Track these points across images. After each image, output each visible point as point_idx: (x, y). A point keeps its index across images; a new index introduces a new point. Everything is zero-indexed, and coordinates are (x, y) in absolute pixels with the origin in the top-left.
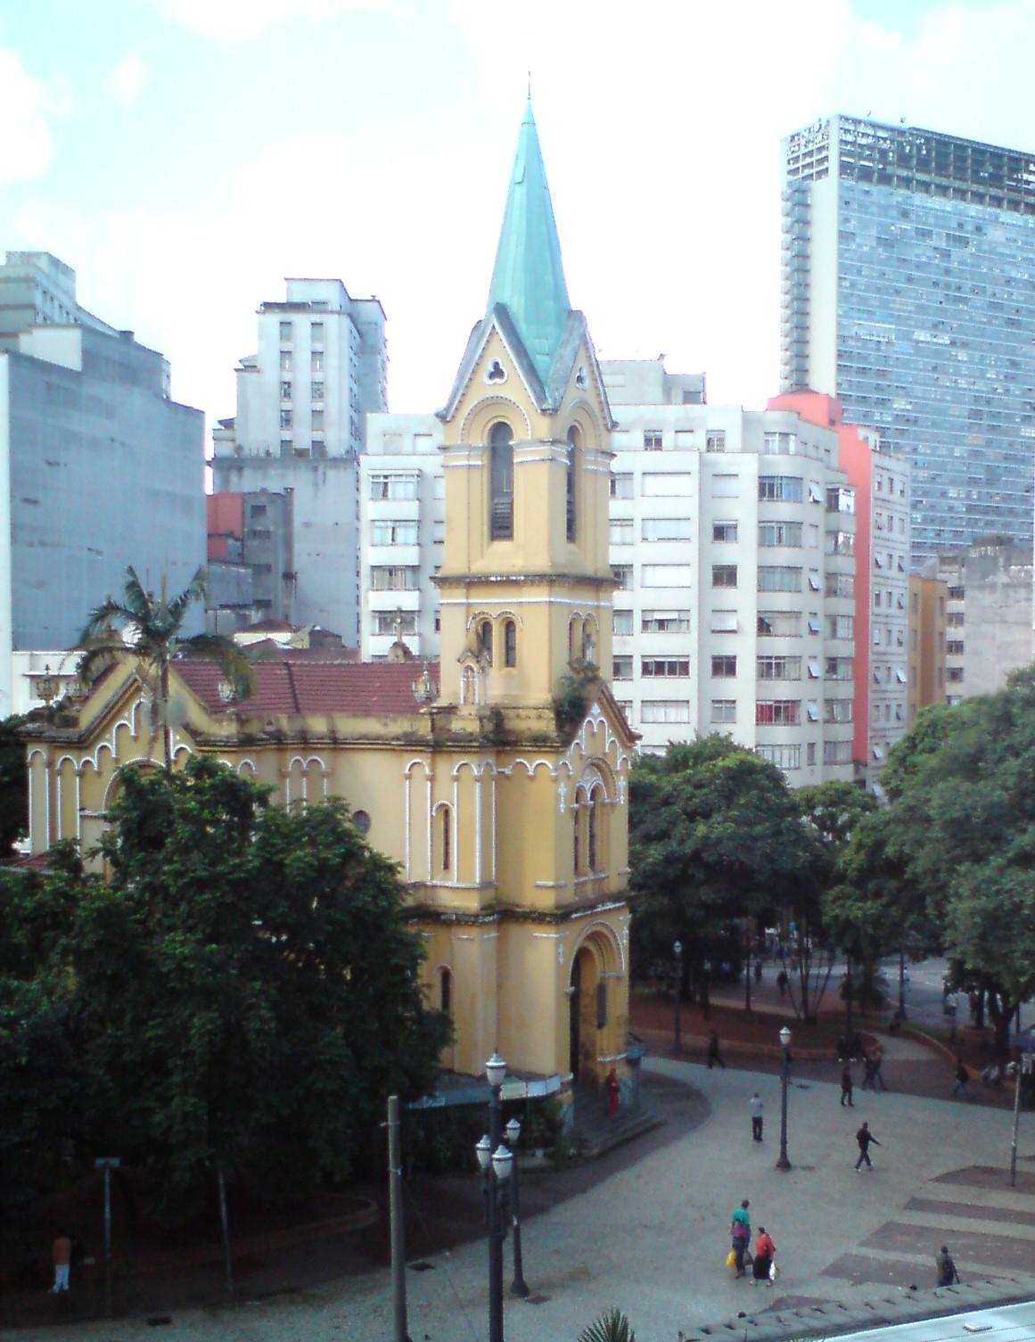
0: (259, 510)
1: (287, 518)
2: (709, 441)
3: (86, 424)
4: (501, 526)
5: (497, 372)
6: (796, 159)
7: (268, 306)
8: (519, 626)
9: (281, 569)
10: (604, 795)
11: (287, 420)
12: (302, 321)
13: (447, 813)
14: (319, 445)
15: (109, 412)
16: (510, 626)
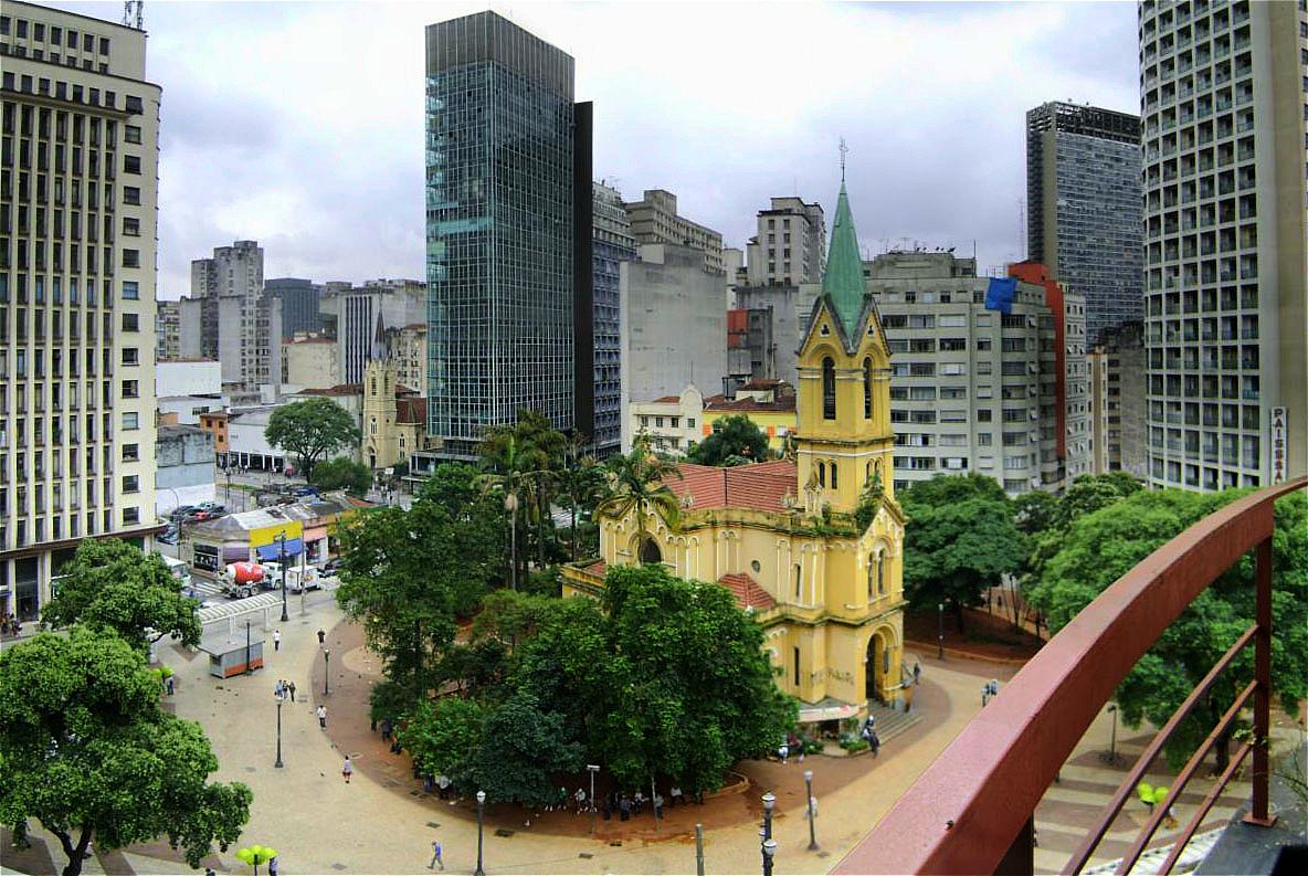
0: (756, 319)
1: (770, 320)
2: (975, 297)
3: (665, 289)
4: (830, 412)
5: (826, 331)
6: (1034, 122)
7: (764, 213)
8: (838, 466)
9: (766, 347)
10: (887, 554)
11: (772, 268)
12: (779, 220)
13: (799, 568)
14: (788, 280)
15: (678, 282)
16: (834, 467)
